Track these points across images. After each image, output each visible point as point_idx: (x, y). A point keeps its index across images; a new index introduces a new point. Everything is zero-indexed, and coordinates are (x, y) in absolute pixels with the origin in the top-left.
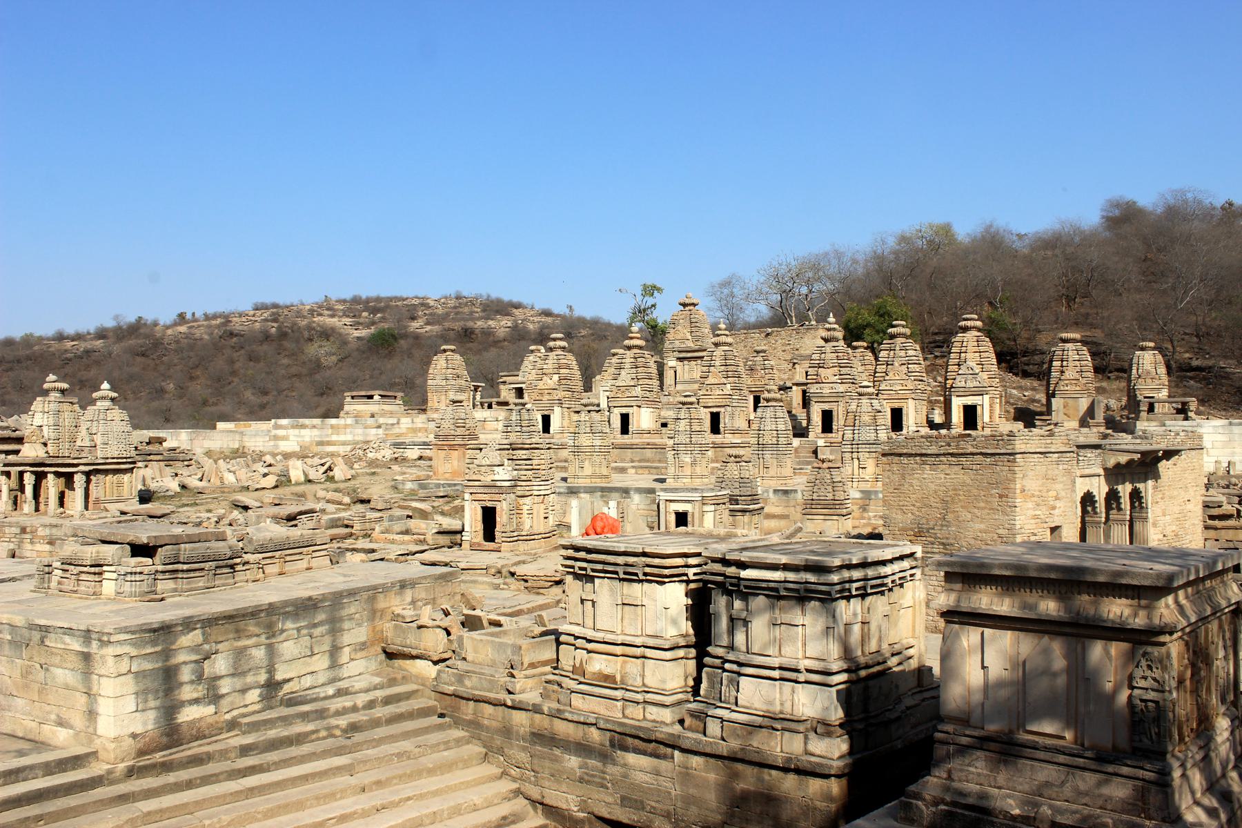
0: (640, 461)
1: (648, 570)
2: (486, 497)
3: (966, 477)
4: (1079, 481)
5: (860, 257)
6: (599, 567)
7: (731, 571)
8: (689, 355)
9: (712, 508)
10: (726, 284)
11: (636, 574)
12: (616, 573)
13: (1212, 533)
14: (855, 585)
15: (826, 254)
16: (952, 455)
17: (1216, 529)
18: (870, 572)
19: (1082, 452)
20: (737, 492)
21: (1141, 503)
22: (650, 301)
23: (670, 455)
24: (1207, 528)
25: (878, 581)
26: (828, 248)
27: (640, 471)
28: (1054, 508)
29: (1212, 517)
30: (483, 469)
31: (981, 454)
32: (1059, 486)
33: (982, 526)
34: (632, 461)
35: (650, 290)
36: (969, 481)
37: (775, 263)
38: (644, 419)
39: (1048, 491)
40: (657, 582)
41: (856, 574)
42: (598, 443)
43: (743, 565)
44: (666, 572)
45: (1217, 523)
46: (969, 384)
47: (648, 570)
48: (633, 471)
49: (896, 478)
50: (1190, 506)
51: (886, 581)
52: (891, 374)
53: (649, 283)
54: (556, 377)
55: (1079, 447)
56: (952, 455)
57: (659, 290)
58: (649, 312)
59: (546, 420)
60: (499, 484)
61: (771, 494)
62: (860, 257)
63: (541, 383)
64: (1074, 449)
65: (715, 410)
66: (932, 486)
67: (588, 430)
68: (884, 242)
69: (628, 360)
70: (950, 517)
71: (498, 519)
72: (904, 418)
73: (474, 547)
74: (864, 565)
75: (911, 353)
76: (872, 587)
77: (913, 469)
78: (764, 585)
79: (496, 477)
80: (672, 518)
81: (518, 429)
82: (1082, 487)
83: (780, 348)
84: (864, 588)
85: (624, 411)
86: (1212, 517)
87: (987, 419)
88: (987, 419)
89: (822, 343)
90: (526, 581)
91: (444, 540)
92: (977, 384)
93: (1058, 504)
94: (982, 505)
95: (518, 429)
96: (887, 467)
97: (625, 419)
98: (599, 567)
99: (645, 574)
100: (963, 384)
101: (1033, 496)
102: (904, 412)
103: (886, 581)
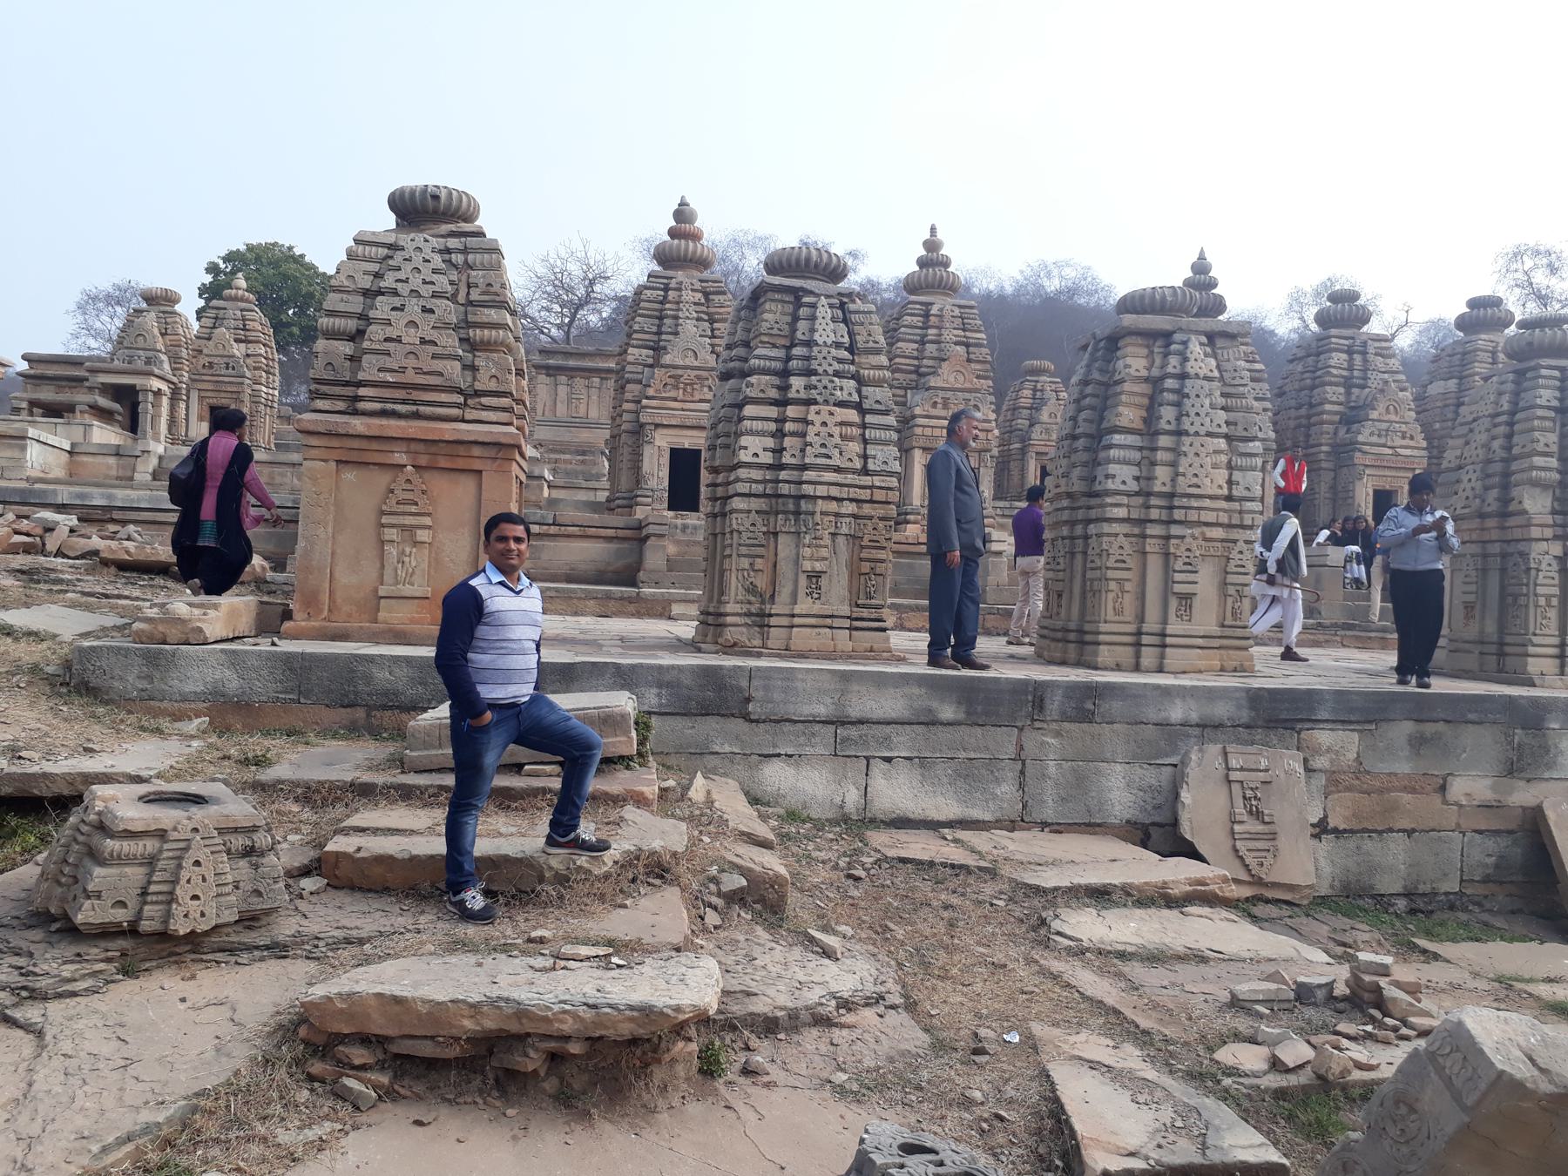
8: (572, 363)
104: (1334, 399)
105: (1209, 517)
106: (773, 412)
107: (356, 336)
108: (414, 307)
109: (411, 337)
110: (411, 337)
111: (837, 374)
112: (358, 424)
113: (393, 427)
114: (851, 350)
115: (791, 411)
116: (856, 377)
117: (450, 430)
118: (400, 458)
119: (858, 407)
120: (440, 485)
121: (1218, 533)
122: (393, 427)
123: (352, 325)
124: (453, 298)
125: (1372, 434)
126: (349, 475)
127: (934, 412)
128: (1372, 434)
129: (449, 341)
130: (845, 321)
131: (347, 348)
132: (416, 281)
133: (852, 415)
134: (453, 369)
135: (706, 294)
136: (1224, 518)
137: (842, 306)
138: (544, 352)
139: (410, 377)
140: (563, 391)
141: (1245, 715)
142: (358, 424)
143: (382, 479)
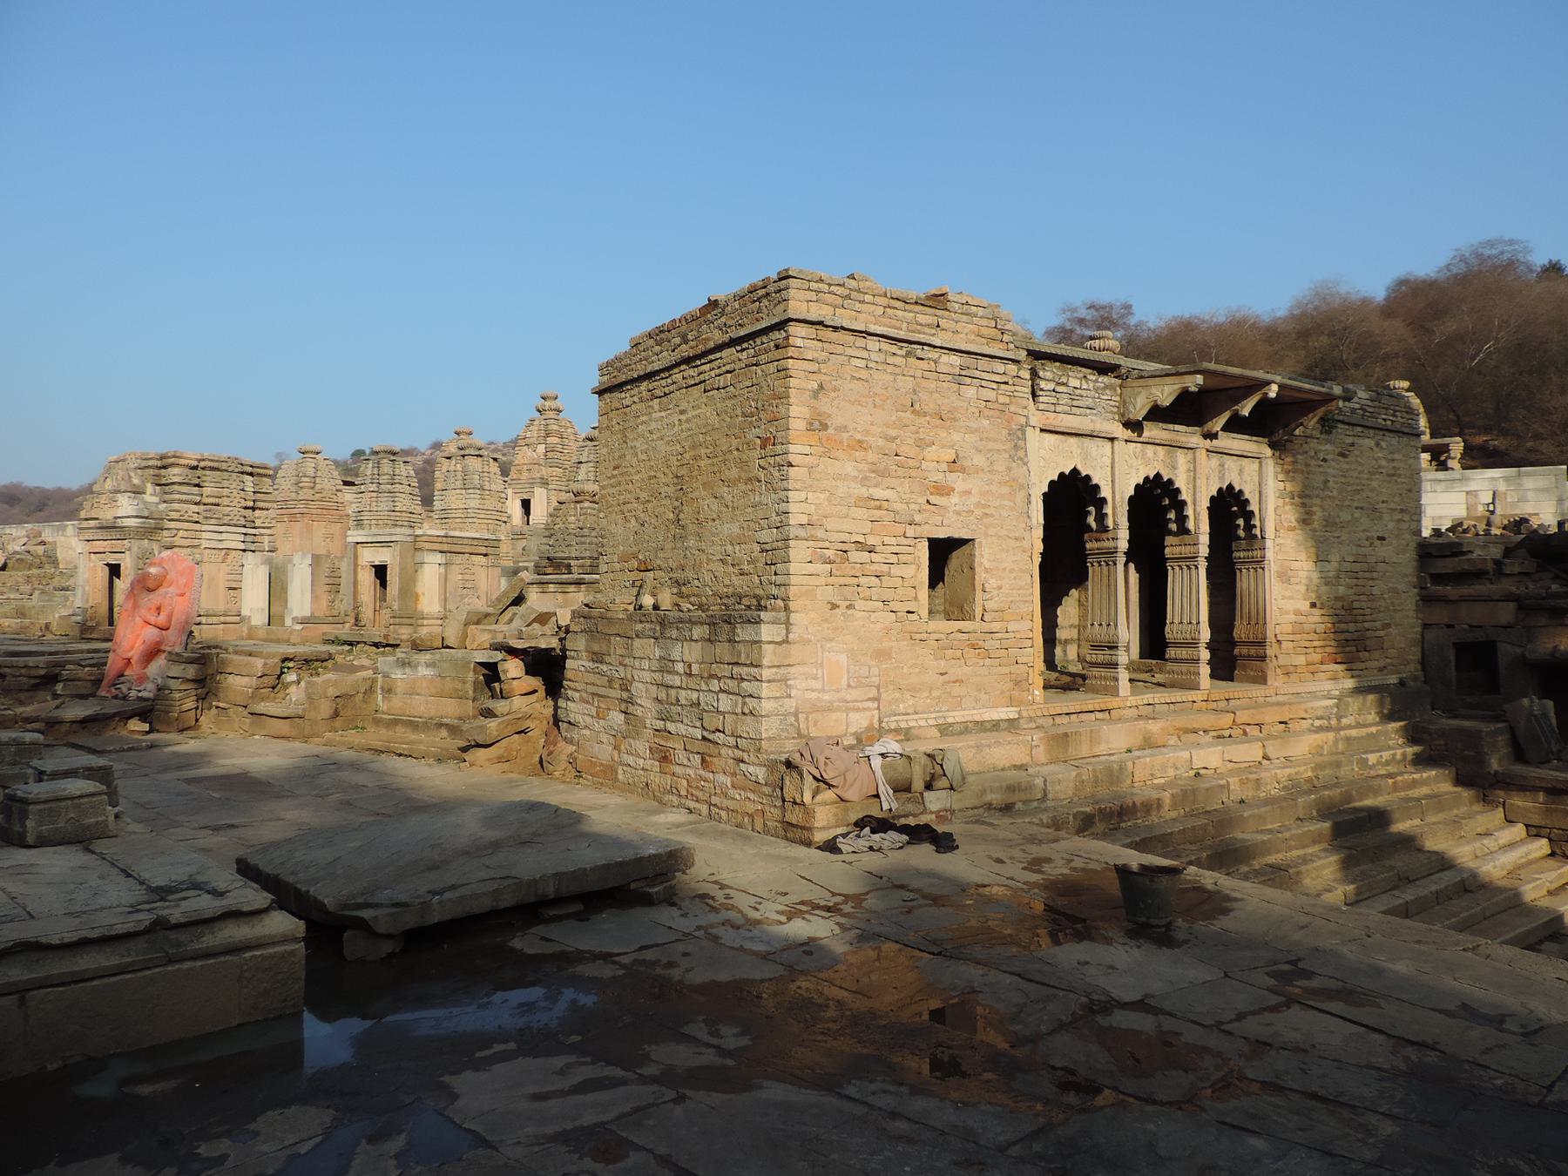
4: (1033, 436)
9: (439, 558)
13: (1440, 614)
16: (687, 361)
17: (1445, 600)
21: (1249, 527)
24: (1426, 600)
28: (944, 490)
29: (1438, 578)
32: (960, 439)
33: (735, 529)
36: (714, 420)
39: (921, 444)
42: (474, 503)
45: (1449, 590)
50: (1383, 551)
54: (541, 449)
55: (1031, 353)
56: (687, 361)
59: (526, 505)
64: (1022, 355)
67: (459, 484)
81: (374, 487)
82: (1048, 461)
86: (1438, 578)
93: (957, 481)
95: (374, 487)
101: (861, 445)
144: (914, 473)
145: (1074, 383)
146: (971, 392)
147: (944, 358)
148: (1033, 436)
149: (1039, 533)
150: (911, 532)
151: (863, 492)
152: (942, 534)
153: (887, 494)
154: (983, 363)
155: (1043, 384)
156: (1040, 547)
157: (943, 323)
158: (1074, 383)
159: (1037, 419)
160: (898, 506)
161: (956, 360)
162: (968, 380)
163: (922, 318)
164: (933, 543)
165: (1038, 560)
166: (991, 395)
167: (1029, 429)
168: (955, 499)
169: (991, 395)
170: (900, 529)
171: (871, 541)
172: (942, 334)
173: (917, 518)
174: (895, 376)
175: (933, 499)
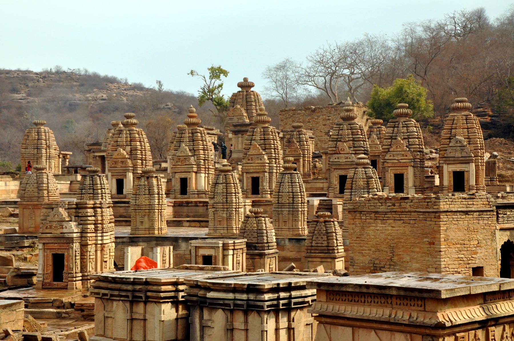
0: (194, 216)
1: (149, 294)
2: (56, 246)
3: (408, 229)
4: (498, 233)
5: (391, 44)
6: (116, 293)
7: (201, 293)
10: (282, 67)
11: (141, 297)
12: (127, 296)
14: (282, 302)
15: (361, 43)
18: (294, 293)
19: (501, 211)
20: (255, 240)
22: (217, 83)
23: (211, 211)
25: (300, 300)
26: (362, 38)
27: (193, 224)
28: (476, 253)
30: (54, 224)
31: (415, 212)
34: (188, 217)
35: (217, 72)
37: (322, 52)
38: (201, 182)
40: (155, 302)
41: (282, 295)
43: (208, 288)
44: (162, 295)
46: (458, 154)
47: (149, 294)
48: (188, 224)
49: (358, 230)
51: (306, 300)
52: (394, 147)
53: (216, 66)
54: (128, 148)
55: (498, 207)
57: (225, 73)
58: (216, 91)
60: (66, 235)
61: (287, 242)
62: (391, 44)
63: (116, 153)
64: (495, 208)
65: (255, 175)
66: (383, 236)
68: (413, 31)
69: (187, 135)
70: (395, 258)
71: (66, 263)
72: (405, 182)
73: (45, 287)
74: (289, 288)
75: (411, 129)
76: (295, 304)
77: (369, 223)
78: (221, 302)
79: (65, 231)
80: (200, 260)
83: (322, 122)
84: (289, 304)
85: (183, 176)
87: (473, 182)
88: (473, 182)
89: (342, 121)
90: (83, 311)
91: (20, 281)
92: (464, 154)
94: (417, 250)
96: (352, 222)
97: (184, 182)
98: (116, 293)
99: (147, 297)
100: (452, 155)
102: (405, 177)
103: (306, 300)
104: (386, 144)
105: (144, 208)
106: (80, 195)
107: (25, 190)
108: (31, 185)
109: (31, 190)
110: (31, 190)
111: (89, 189)
112: (25, 203)
113: (29, 203)
114: (93, 184)
115: (82, 195)
116: (93, 189)
117: (36, 203)
118: (30, 207)
119: (93, 194)
120: (35, 210)
121: (148, 211)
122: (29, 203)
123: (24, 189)
124: (37, 183)
125: (390, 156)
126: (25, 210)
127: (249, 162)
128: (390, 156)
129: (36, 190)
130: (92, 180)
131: (24, 192)
132: (32, 182)
133: (92, 195)
134: (36, 194)
135: (192, 133)
136: (148, 208)
137: (92, 178)
138: (235, 126)
139: (31, 196)
140: (240, 139)
141: (128, 241)
142: (25, 203)
143: (29, 210)
144: (469, 249)
145: (508, 213)
146: (481, 222)
147: (475, 214)
148: (498, 233)
149: (500, 262)
150: (468, 266)
151: (457, 256)
152: (475, 266)
153: (462, 256)
154: (485, 213)
155: (500, 216)
156: (500, 266)
157: (474, 203)
158: (508, 213)
159: (498, 227)
160: (465, 259)
161: (478, 213)
162: (480, 219)
163: (470, 203)
164: (473, 268)
165: (499, 270)
166: (486, 222)
167: (496, 231)
168: (478, 255)
169: (486, 222)
170: (465, 266)
171: (459, 270)
172: (475, 206)
173: (470, 262)
174: (464, 221)
175: (474, 256)
